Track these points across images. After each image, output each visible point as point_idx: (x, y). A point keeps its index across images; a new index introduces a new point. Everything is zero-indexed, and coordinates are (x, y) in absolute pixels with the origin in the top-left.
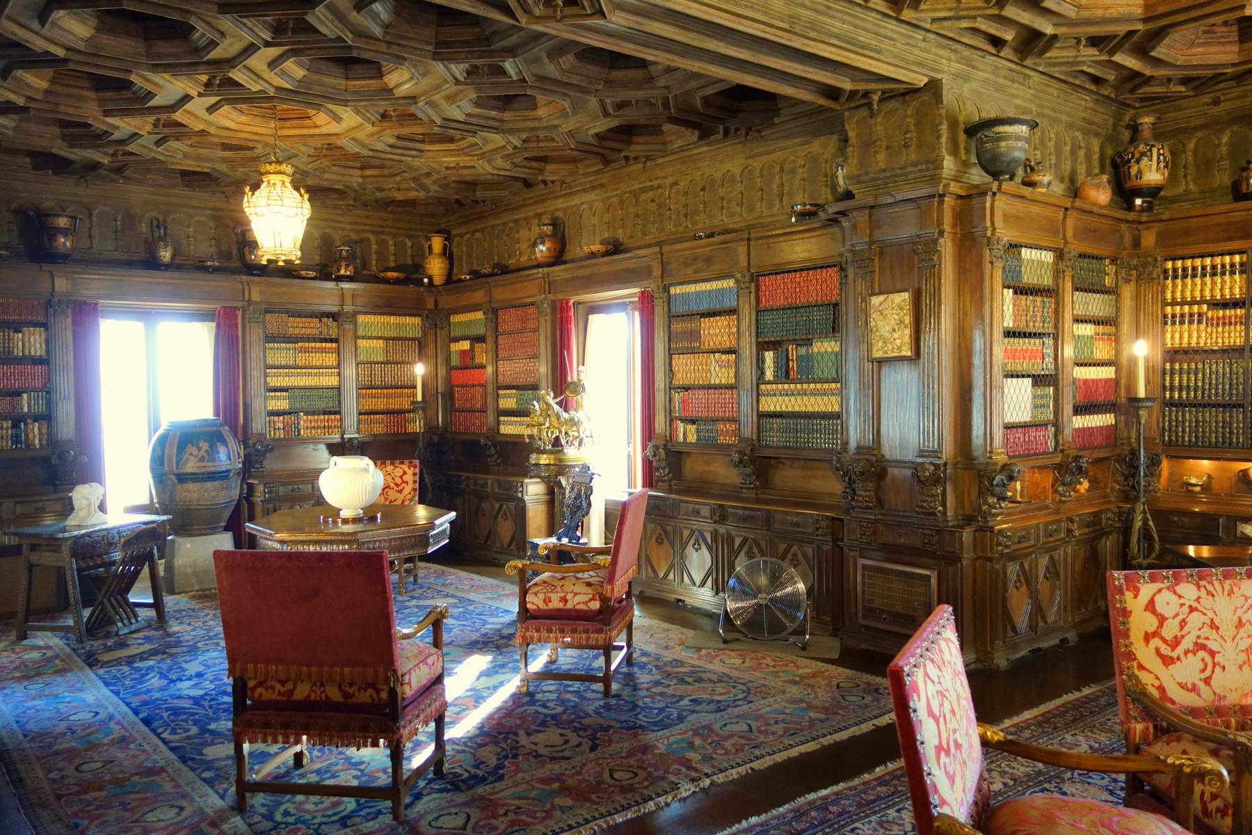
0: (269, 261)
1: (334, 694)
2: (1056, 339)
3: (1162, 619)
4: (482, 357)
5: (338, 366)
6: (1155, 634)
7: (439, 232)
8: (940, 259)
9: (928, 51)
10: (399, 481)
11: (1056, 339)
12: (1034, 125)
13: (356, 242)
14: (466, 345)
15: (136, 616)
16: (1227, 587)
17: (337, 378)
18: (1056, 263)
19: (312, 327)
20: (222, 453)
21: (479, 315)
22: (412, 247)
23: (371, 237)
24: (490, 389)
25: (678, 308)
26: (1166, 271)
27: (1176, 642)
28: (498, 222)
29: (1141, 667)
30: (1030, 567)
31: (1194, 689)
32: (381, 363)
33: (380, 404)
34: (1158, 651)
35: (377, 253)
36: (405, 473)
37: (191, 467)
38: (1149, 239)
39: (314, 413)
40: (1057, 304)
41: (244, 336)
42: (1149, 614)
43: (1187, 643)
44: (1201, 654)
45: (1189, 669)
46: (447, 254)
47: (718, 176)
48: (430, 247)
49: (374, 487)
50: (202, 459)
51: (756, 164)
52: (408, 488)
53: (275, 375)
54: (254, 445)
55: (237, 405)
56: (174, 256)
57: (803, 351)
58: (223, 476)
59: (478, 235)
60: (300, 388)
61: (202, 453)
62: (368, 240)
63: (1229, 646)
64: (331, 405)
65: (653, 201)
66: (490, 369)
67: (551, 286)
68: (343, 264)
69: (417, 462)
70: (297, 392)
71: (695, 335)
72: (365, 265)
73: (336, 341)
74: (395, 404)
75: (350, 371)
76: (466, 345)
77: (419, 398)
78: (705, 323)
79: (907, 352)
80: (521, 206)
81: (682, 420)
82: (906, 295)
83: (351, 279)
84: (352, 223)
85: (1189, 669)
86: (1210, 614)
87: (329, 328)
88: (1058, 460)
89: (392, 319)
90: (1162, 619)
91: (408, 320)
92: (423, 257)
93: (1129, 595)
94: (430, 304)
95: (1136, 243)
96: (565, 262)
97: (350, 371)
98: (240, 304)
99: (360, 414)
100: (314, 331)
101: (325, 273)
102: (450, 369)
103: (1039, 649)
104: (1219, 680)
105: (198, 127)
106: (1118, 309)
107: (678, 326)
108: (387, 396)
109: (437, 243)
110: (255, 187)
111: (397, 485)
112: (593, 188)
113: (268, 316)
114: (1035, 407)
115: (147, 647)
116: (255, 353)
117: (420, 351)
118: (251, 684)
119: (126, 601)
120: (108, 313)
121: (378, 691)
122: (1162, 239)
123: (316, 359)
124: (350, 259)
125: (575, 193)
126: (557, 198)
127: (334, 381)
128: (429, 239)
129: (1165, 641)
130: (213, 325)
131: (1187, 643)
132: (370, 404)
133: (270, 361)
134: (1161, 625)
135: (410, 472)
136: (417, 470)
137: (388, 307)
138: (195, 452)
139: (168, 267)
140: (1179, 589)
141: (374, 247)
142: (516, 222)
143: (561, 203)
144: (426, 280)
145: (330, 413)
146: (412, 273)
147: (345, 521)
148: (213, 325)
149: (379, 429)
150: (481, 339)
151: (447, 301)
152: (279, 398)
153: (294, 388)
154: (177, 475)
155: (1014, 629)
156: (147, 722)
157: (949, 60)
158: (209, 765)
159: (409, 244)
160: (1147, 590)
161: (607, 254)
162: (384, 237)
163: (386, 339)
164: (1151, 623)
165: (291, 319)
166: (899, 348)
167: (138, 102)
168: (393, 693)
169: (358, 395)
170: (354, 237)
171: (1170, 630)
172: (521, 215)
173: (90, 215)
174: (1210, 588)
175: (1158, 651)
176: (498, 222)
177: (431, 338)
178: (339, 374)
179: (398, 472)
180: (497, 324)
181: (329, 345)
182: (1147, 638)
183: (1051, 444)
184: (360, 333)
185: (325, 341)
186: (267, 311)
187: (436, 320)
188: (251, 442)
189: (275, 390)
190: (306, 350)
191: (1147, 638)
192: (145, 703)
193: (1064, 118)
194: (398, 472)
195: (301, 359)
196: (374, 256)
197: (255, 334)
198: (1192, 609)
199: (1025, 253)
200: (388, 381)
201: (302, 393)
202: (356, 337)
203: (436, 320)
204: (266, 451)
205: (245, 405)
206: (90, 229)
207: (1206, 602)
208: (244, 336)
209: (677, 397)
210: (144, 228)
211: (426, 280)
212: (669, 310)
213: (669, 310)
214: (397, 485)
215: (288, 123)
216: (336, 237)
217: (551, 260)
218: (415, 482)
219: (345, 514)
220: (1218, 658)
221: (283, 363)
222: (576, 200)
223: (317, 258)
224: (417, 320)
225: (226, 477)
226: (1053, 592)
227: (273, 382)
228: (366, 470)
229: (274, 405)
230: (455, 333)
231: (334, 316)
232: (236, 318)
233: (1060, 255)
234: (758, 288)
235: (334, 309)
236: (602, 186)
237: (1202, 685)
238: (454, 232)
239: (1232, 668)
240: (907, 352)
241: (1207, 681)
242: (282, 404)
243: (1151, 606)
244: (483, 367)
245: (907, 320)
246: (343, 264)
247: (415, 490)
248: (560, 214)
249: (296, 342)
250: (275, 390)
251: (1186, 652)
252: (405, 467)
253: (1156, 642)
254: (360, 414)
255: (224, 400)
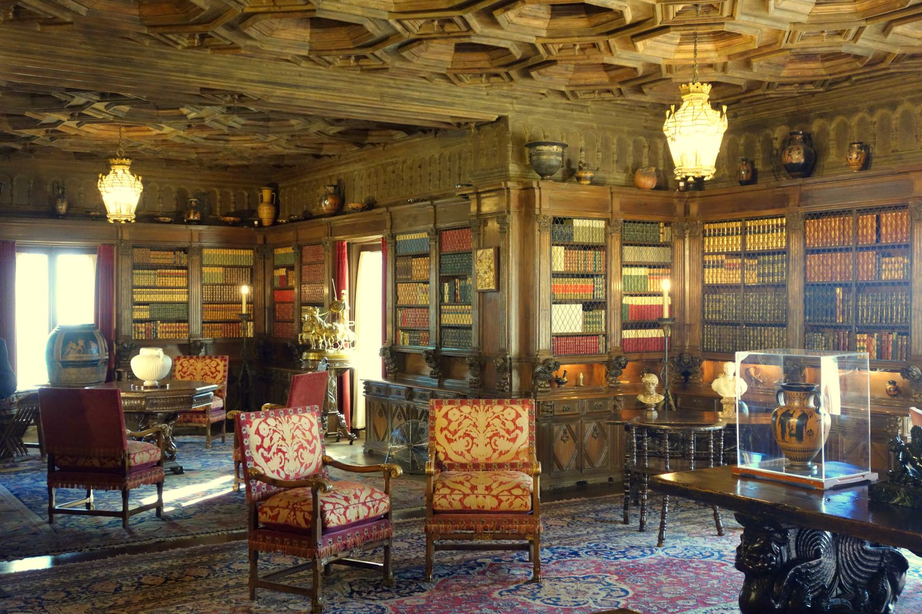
0: (115, 221)
1: (96, 463)
2: (606, 278)
3: (450, 422)
4: (293, 282)
5: (187, 287)
6: (445, 429)
7: (269, 186)
8: (508, 228)
9: (494, 101)
10: (213, 370)
11: (606, 278)
12: (564, 146)
13: (204, 194)
14: (282, 272)
15: (26, 452)
16: (486, 408)
17: (186, 296)
18: (606, 228)
19: (168, 258)
20: (94, 348)
21: (290, 250)
22: (249, 197)
23: (216, 190)
24: (296, 305)
25: (401, 251)
26: (704, 231)
27: (456, 432)
28: (306, 180)
29: (438, 444)
30: (577, 429)
31: (462, 454)
32: (221, 285)
33: (220, 316)
34: (446, 436)
35: (221, 202)
36: (218, 365)
37: (72, 357)
38: (694, 209)
39: (170, 321)
40: (606, 256)
41: (117, 264)
42: (444, 419)
43: (461, 433)
44: (467, 438)
45: (460, 445)
46: (275, 203)
47: (427, 158)
48: (262, 196)
49: (163, 367)
50: (79, 351)
51: (447, 153)
52: (220, 376)
53: (139, 293)
54: (123, 344)
55: (111, 315)
56: (69, 208)
57: (463, 282)
58: (93, 364)
59: (295, 189)
60: (162, 303)
61: (79, 347)
62: (214, 192)
63: (481, 436)
64: (182, 315)
65: (394, 172)
66: (296, 290)
67: (332, 232)
68: (192, 211)
69: (227, 357)
70: (155, 306)
71: (408, 270)
72: (211, 211)
73: (186, 268)
74: (232, 316)
75: (196, 290)
76: (282, 272)
77: (244, 311)
78: (415, 262)
79: (493, 287)
80: (320, 170)
81: (403, 330)
82: (492, 250)
83: (199, 223)
84: (201, 180)
85: (460, 445)
86: (474, 420)
87: (181, 258)
88: (606, 358)
89: (230, 252)
90: (450, 422)
91: (242, 252)
92: (257, 204)
93: (437, 410)
94: (260, 241)
95: (687, 211)
96: (345, 213)
97: (196, 290)
98: (114, 242)
99: (204, 322)
100: (170, 261)
101: (179, 218)
102: (274, 289)
103: (585, 482)
104: (475, 451)
105: (73, 133)
106: (672, 257)
107: (400, 263)
108: (225, 310)
109: (266, 194)
110: (106, 173)
111: (212, 373)
112: (360, 160)
113: (136, 250)
114: (585, 323)
115: (29, 467)
116: (125, 277)
117: (252, 276)
118: (57, 457)
119: (22, 445)
120: (23, 249)
121: (117, 461)
122: (703, 209)
123: (171, 282)
124: (196, 209)
125: (348, 163)
126: (340, 165)
127: (184, 298)
128: (261, 191)
129: (450, 432)
130: (96, 256)
131: (461, 433)
132: (210, 316)
133: (136, 283)
134: (449, 424)
135: (222, 364)
136: (227, 363)
137: (228, 243)
138: (74, 346)
139: (64, 216)
140: (462, 408)
141: (219, 197)
142: (317, 180)
143: (343, 170)
144: (256, 223)
145: (180, 321)
146: (247, 217)
147: (146, 388)
148: (96, 256)
149: (218, 334)
150: (290, 268)
151: (272, 238)
152: (141, 310)
153: (153, 303)
154: (62, 363)
155: (560, 466)
156: (16, 495)
157: (512, 103)
158: (42, 510)
159: (246, 194)
160: (445, 408)
161: (363, 209)
162: (227, 190)
163: (224, 266)
164: (444, 423)
165: (153, 252)
166: (489, 284)
167: (34, 123)
168: (124, 462)
169: (202, 308)
170: (203, 190)
171: (453, 427)
172: (318, 176)
173: (12, 180)
174: (477, 408)
175: (446, 436)
176: (306, 180)
177: (260, 266)
178: (188, 293)
179: (214, 364)
180: (301, 257)
181: (180, 271)
182: (442, 430)
183: (602, 349)
184: (204, 262)
185: (178, 268)
186: (134, 247)
187: (264, 252)
188: (120, 342)
189: (140, 304)
190: (164, 275)
191: (442, 430)
192: (18, 489)
193: (626, 129)
194: (214, 364)
195: (160, 282)
196: (218, 205)
197: (126, 263)
198: (466, 418)
199: (577, 223)
200: (226, 298)
201: (159, 306)
202: (202, 265)
203: (264, 252)
204: (131, 348)
205: (117, 314)
206: (11, 190)
207: (474, 414)
208: (117, 264)
209: (400, 314)
210: (48, 188)
211: (256, 223)
212: (396, 252)
213: (396, 252)
214: (212, 373)
215: (132, 129)
216: (189, 191)
217: (333, 212)
218: (225, 371)
219: (147, 383)
220: (475, 441)
221: (146, 284)
222: (351, 168)
223: (174, 207)
224: (249, 253)
225: (96, 365)
226: (601, 447)
227: (138, 298)
228: (159, 356)
229: (137, 315)
230: (277, 263)
231: (185, 250)
232: (112, 251)
233: (608, 222)
234: (440, 238)
235: (186, 245)
236: (365, 159)
237: (466, 453)
238: (280, 185)
239: (482, 445)
240: (493, 287)
241: (469, 451)
242: (145, 315)
243: (446, 416)
244: (292, 289)
245: (492, 266)
246: (192, 211)
247: (224, 377)
248: (342, 177)
249: (156, 269)
250: (140, 304)
251: (460, 437)
252: (218, 360)
253: (446, 432)
254: (204, 322)
255: (102, 310)
